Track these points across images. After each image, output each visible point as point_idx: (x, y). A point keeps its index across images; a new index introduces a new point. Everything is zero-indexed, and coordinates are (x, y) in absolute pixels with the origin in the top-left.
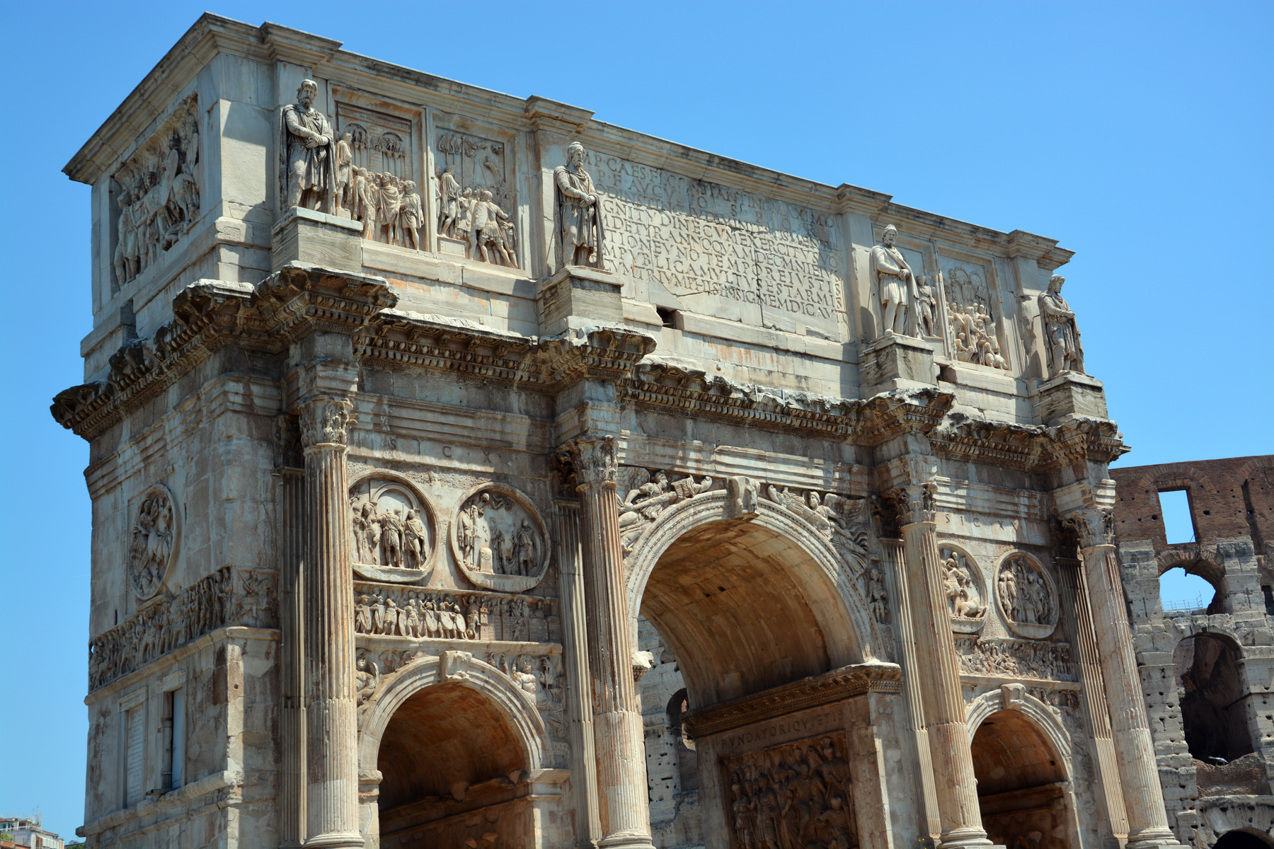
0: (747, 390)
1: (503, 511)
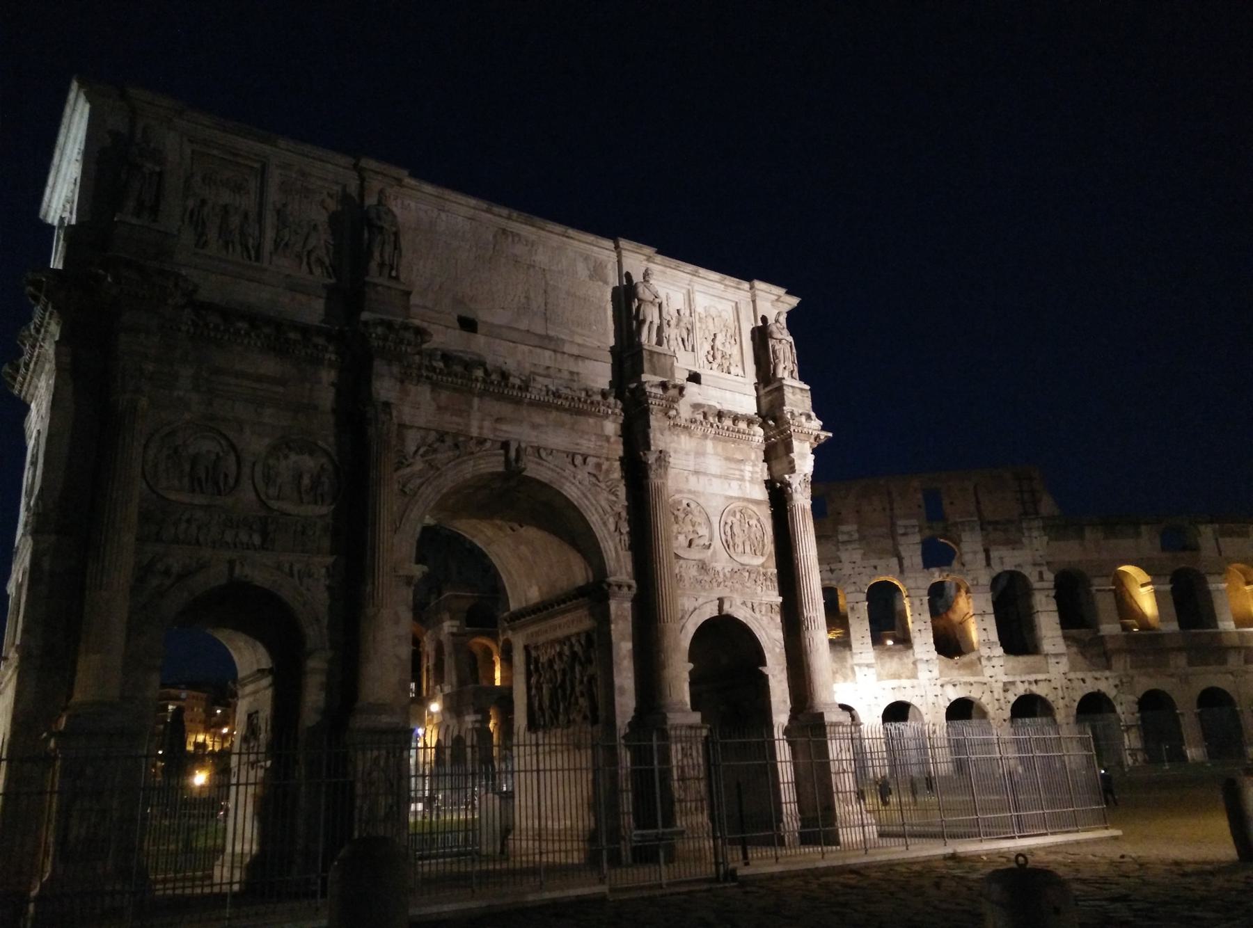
0: (524, 378)
1: (306, 457)
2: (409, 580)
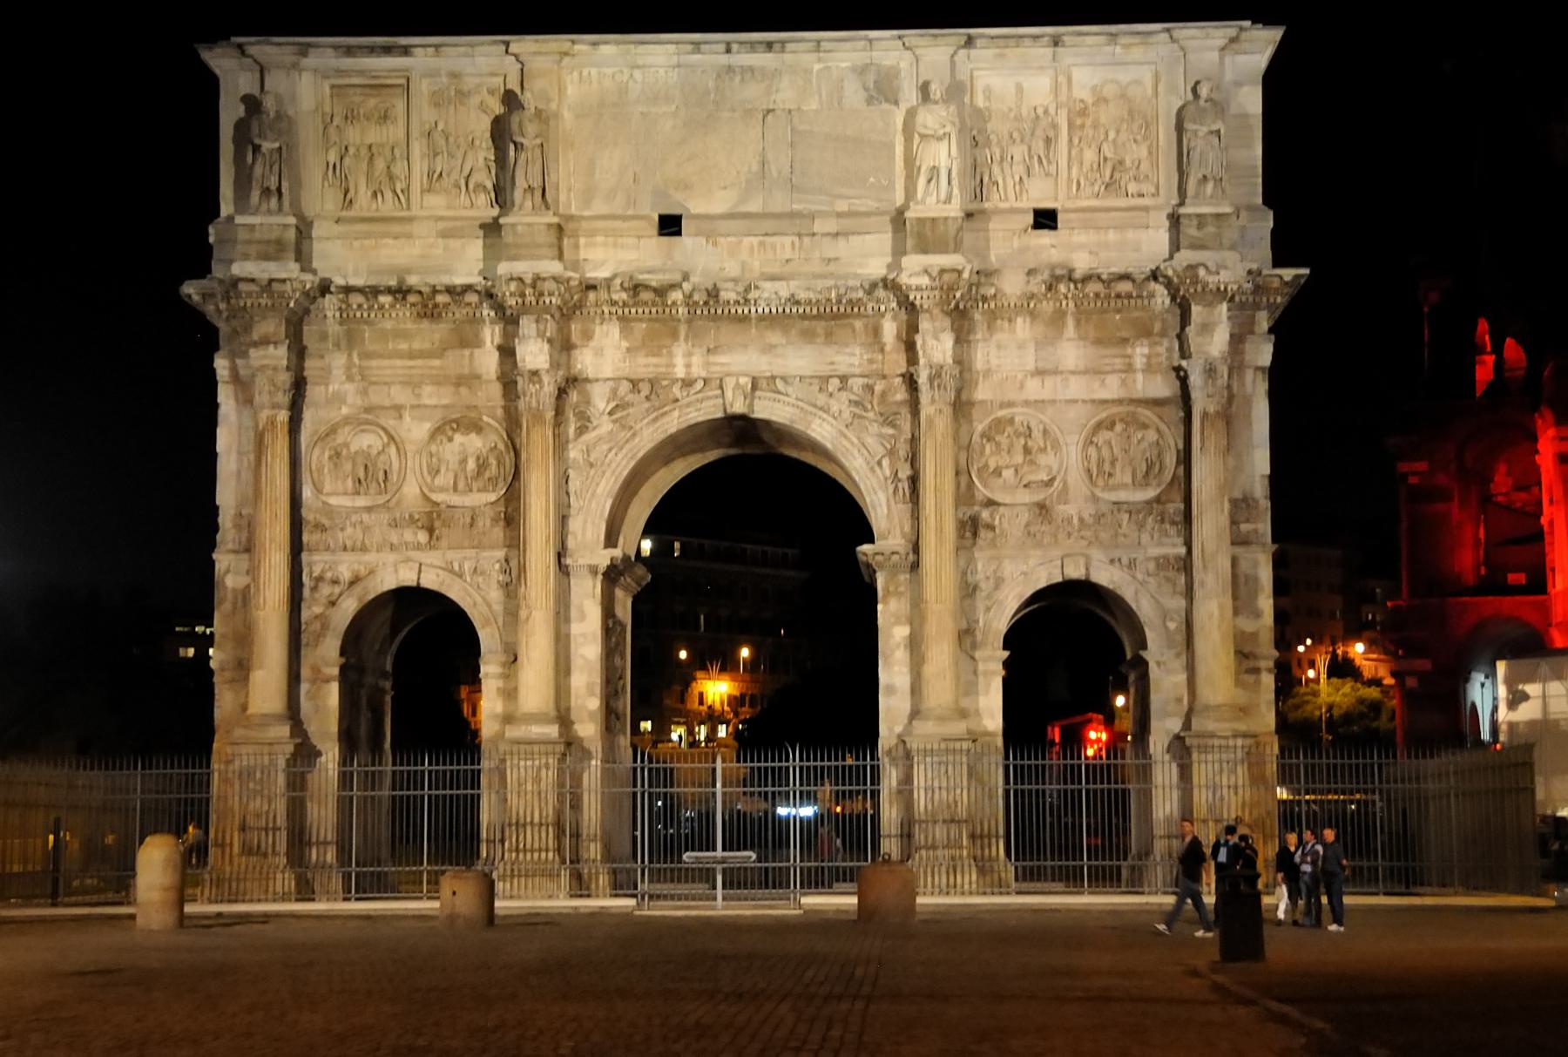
1: (473, 436)
2: (593, 570)
